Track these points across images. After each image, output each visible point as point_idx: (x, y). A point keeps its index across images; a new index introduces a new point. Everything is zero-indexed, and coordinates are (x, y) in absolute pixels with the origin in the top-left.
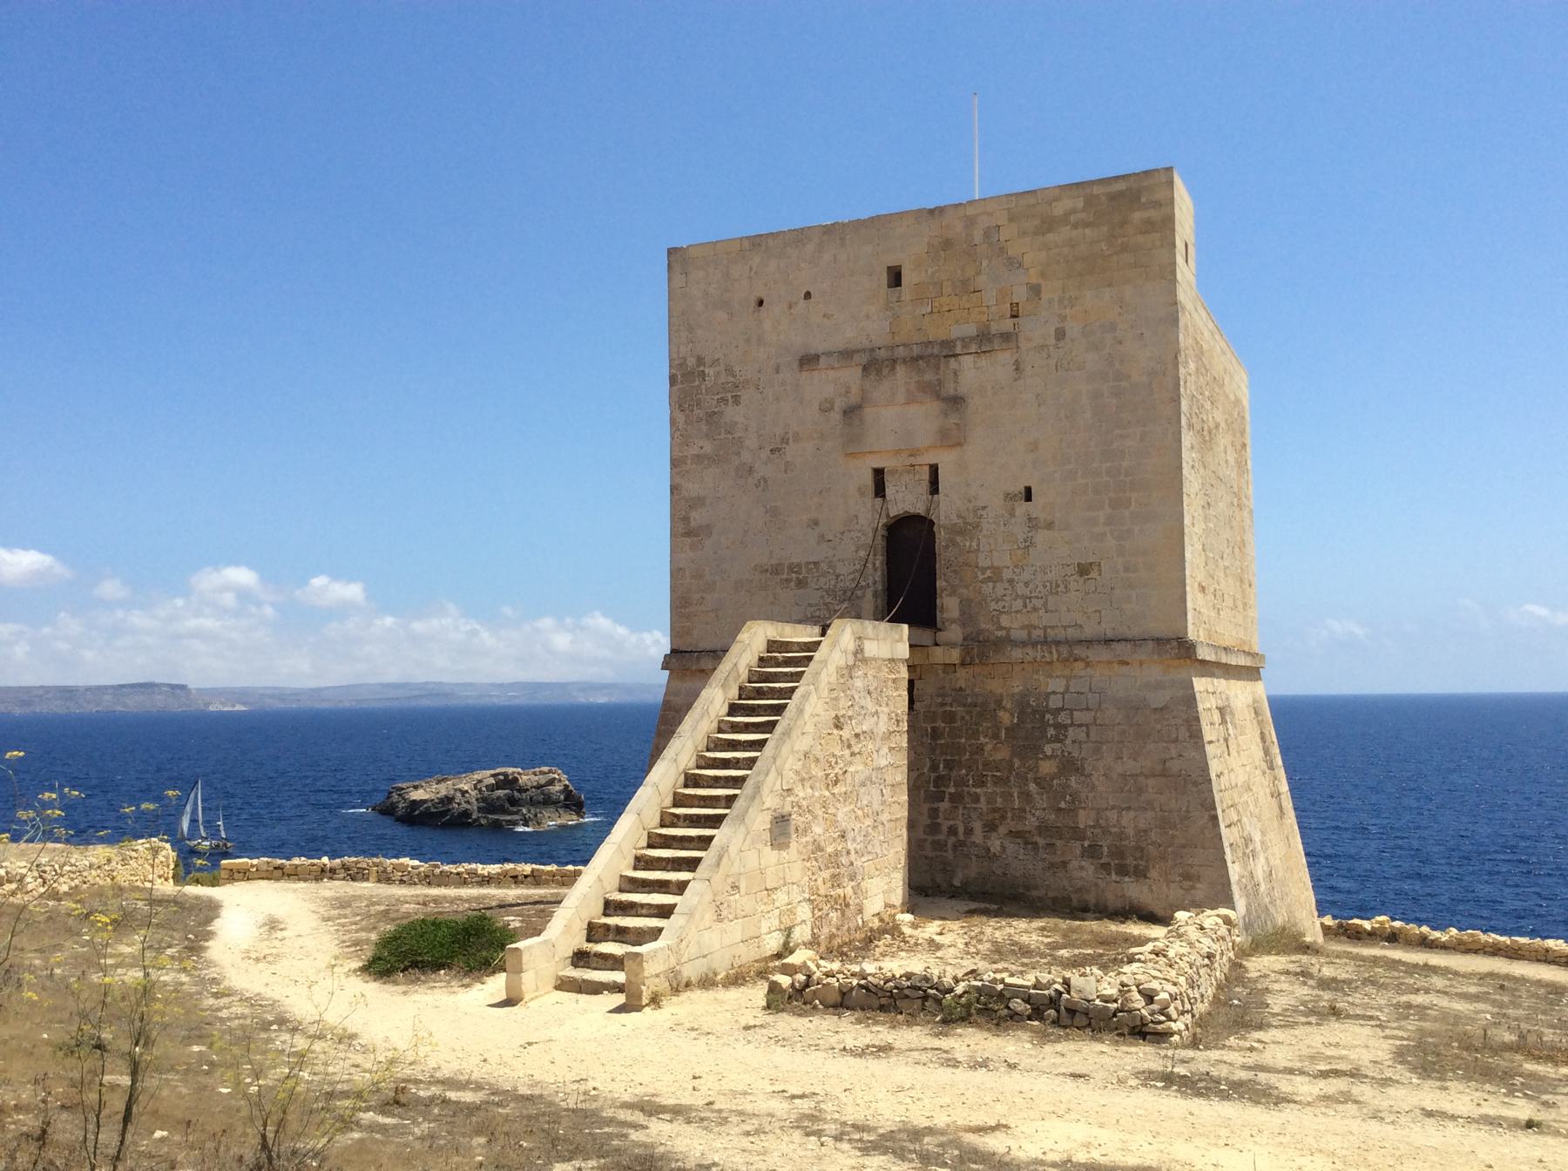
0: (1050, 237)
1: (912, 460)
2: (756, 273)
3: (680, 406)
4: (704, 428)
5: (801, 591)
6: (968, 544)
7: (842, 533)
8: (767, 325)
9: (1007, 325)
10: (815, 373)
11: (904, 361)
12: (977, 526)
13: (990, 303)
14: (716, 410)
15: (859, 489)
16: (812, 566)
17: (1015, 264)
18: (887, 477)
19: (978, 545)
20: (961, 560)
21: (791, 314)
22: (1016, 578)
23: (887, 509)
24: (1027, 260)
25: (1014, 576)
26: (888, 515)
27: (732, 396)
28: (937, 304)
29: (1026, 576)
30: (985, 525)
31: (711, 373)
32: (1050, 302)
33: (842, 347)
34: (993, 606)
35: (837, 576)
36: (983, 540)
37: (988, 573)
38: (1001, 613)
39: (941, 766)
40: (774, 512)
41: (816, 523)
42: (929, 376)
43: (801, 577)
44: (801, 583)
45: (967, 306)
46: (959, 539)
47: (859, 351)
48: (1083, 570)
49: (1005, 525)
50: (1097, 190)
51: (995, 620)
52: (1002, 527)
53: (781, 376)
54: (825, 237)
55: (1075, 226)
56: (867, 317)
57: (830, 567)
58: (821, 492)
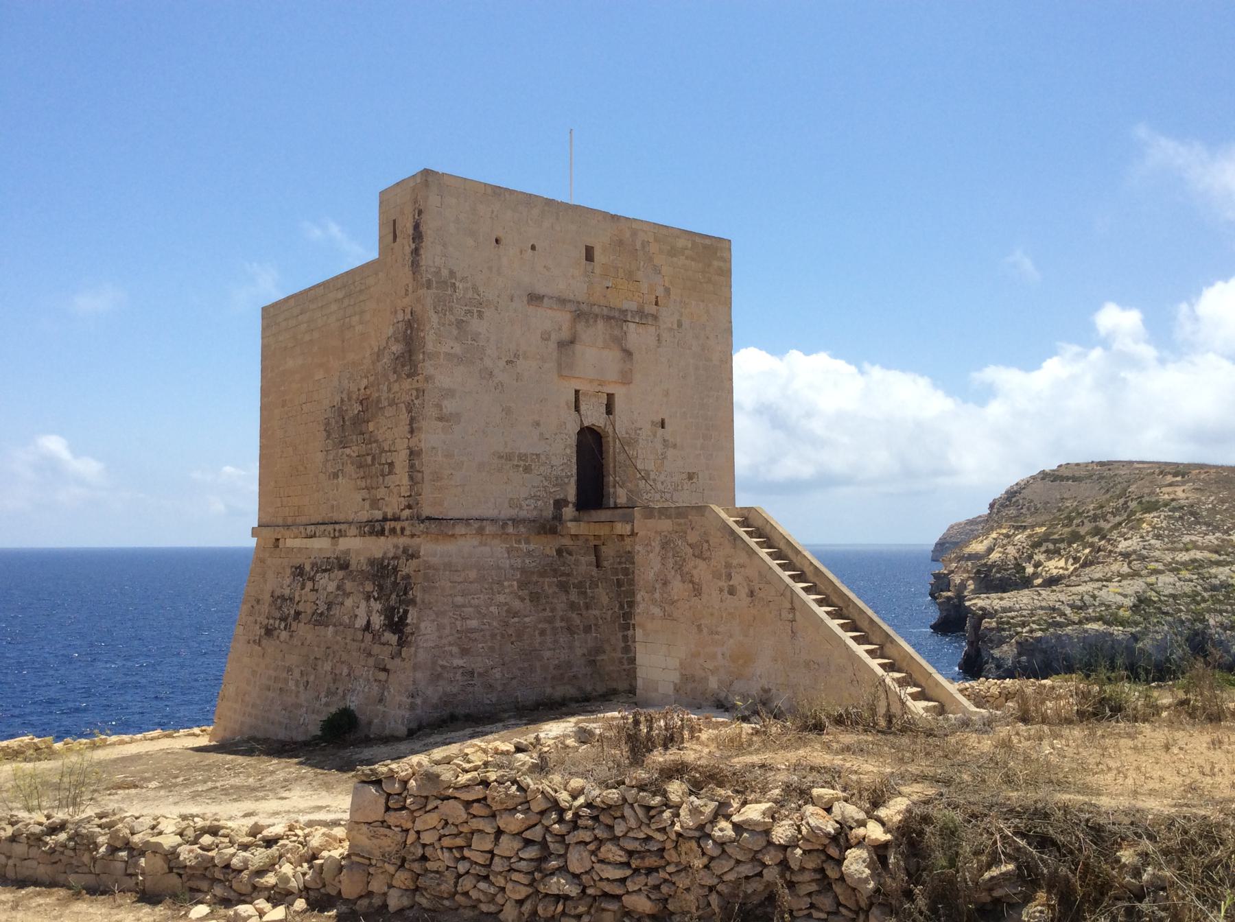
1: (599, 388)
2: (497, 216)
3: (435, 308)
4: (455, 332)
5: (527, 475)
7: (556, 434)
14: (464, 319)
15: (567, 404)
16: (535, 457)
17: (657, 270)
18: (581, 397)
27: (477, 311)
29: (662, 478)
31: (461, 287)
34: (645, 496)
35: (552, 466)
39: (626, 606)
40: (508, 411)
41: (538, 424)
42: (617, 332)
44: (527, 469)
47: (570, 301)
48: (690, 477)
50: (698, 240)
54: (546, 208)
55: (687, 258)
56: (573, 276)
57: (547, 458)
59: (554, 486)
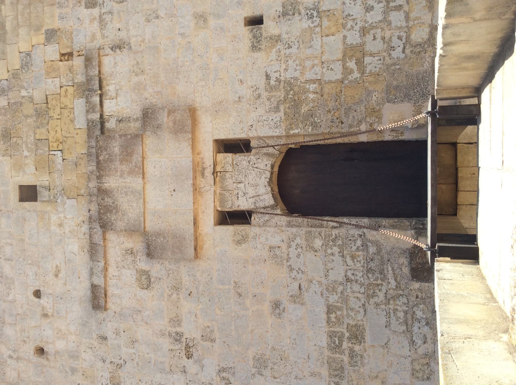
0: (8, 26)
2: (14, 351)
5: (368, 337)
6: (311, 96)
7: (291, 269)
8: (60, 345)
9: (78, 62)
10: (111, 291)
11: (99, 177)
12: (290, 84)
13: (58, 86)
15: (239, 243)
16: (333, 316)
18: (228, 207)
19: (313, 81)
20: (331, 104)
21: (52, 315)
22: (360, 24)
23: (264, 208)
24: (24, 47)
25: (357, 28)
26: (272, 207)
28: (55, 145)
29: (357, 10)
30: (289, 75)
32: (62, 18)
33: (86, 257)
34: (397, 53)
35: (348, 280)
36: (309, 75)
37: (352, 64)
38: (408, 37)
41: (276, 305)
42: (116, 147)
43: (347, 335)
45: (58, 110)
46: (304, 109)
47: (91, 236)
49: (290, 47)
51: (418, 49)
52: (294, 50)
53: (110, 335)
56: (60, 225)
57: (334, 289)
58: (240, 295)
59: (384, 278)
